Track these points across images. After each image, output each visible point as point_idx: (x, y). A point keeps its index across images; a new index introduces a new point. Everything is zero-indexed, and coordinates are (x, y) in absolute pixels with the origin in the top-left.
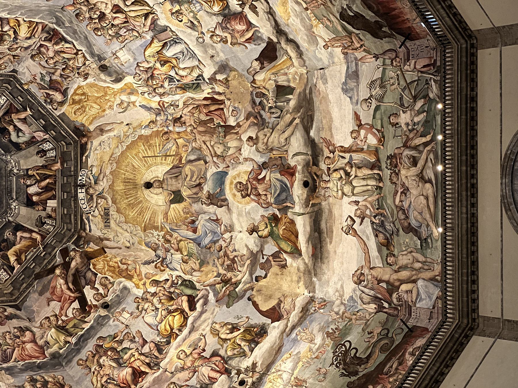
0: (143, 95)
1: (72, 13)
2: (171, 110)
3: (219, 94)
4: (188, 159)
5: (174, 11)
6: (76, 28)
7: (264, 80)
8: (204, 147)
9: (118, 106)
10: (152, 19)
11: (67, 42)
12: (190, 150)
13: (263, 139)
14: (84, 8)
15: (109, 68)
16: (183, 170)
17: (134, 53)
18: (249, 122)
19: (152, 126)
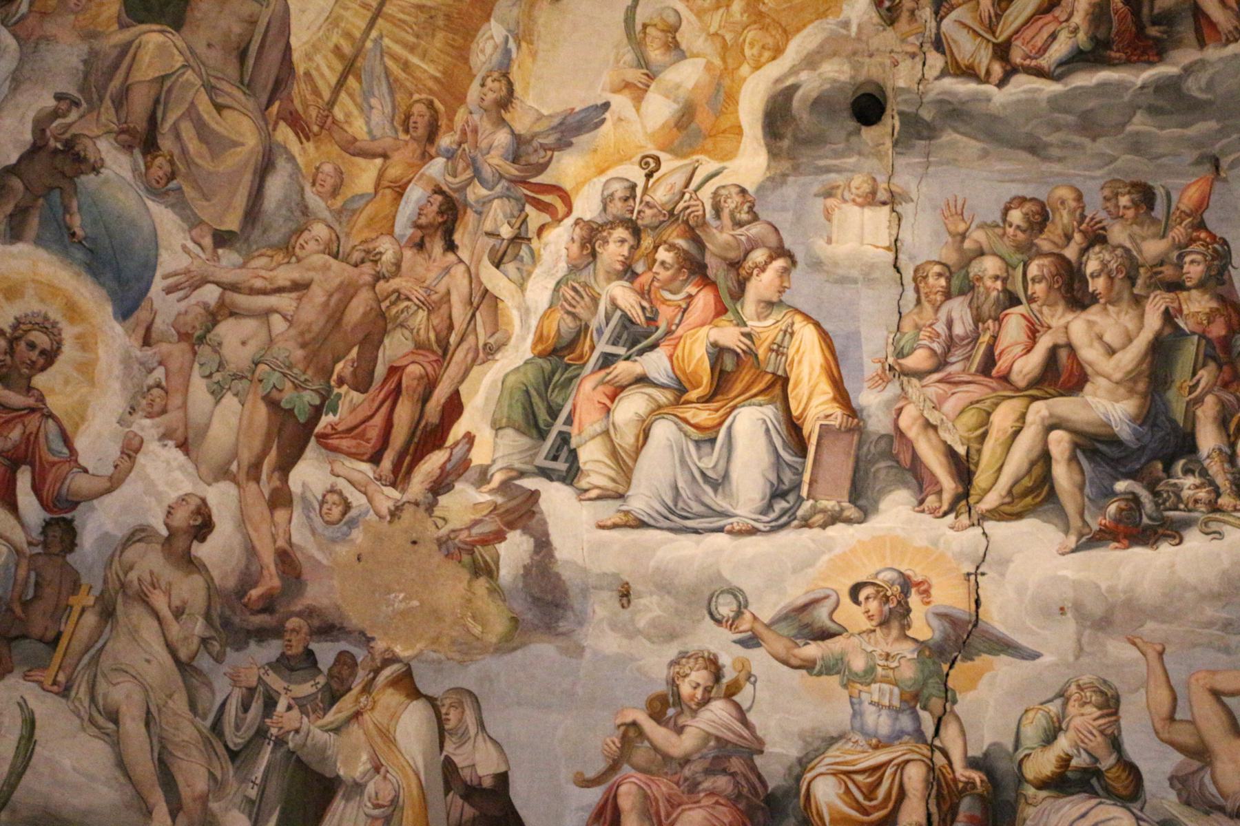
0: (643, 161)
1: (1172, 182)
2: (499, 219)
3: (440, 486)
4: (281, 163)
5: (914, 600)
6: (1102, 145)
7: (388, 737)
8: (285, 275)
9: (672, 19)
10: (935, 481)
11: (1079, 59)
12: (314, 200)
13: (168, 593)
14: (1153, 248)
15: (852, 124)
16: (250, 104)
17: (843, 280)
18: (268, 558)
19: (495, 89)
